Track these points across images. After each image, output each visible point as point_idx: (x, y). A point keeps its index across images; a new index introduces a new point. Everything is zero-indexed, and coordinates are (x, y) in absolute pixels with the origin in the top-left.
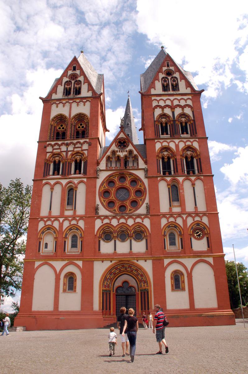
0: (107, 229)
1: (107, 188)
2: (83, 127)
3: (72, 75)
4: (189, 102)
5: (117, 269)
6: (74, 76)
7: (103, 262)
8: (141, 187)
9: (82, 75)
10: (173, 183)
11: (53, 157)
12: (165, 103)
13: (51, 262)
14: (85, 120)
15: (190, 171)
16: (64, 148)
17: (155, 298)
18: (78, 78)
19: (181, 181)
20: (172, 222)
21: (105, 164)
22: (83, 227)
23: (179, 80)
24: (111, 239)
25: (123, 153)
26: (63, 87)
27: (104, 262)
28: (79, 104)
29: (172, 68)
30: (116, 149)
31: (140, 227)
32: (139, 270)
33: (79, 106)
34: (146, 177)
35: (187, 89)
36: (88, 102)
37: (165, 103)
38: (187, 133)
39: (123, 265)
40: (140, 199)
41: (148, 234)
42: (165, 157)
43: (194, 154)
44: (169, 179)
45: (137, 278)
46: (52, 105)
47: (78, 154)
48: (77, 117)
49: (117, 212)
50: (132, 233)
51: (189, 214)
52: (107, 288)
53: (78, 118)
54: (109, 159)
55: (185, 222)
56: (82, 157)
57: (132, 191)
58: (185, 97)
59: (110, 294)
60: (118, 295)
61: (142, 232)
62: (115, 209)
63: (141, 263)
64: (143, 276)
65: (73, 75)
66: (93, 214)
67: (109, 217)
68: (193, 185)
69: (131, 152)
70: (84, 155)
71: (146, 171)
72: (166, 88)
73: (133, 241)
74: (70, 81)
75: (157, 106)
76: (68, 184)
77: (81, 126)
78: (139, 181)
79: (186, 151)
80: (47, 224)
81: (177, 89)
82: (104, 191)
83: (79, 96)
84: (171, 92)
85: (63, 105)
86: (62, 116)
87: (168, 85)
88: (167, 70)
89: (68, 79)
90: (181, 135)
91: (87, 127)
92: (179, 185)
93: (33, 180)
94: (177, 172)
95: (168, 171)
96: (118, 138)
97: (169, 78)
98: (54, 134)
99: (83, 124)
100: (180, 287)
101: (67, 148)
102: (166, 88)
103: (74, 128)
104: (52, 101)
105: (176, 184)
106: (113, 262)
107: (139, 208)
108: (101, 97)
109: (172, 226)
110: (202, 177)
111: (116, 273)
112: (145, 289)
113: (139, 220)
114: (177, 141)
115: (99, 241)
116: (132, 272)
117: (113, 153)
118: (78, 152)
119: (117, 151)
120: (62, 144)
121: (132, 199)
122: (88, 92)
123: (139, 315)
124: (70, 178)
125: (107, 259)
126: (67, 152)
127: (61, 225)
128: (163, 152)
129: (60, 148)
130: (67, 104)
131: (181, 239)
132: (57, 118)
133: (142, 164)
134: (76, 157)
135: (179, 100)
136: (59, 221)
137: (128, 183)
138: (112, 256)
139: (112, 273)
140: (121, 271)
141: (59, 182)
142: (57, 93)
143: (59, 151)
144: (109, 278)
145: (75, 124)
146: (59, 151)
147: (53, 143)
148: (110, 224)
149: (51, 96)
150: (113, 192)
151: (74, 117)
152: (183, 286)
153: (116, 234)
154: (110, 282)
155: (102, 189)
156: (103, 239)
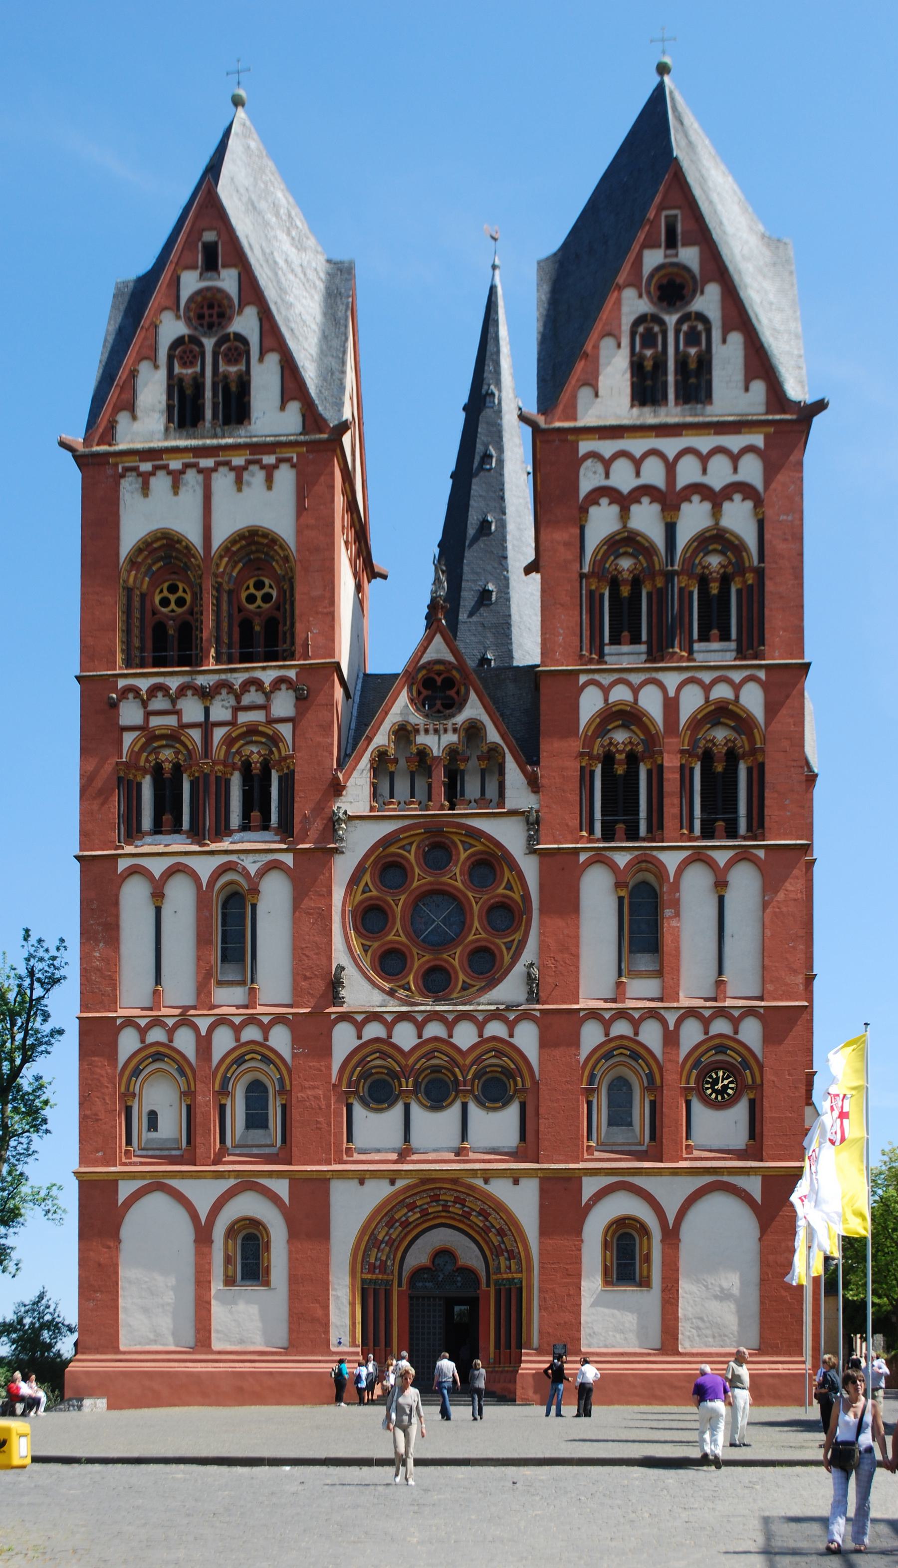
0: (379, 1062)
1: (375, 893)
2: (267, 598)
3: (199, 299)
5: (412, 1207)
6: (211, 306)
7: (362, 1182)
9: (249, 303)
10: (640, 876)
11: (149, 749)
12: (638, 474)
14: (274, 564)
15: (716, 820)
16: (192, 710)
18: (230, 319)
19: (672, 871)
20: (622, 1037)
21: (366, 791)
22: (286, 1054)
23: (716, 334)
26: (162, 374)
27: (367, 1182)
29: (689, 256)
31: (500, 1053)
32: (490, 1215)
33: (244, 488)
34: (532, 851)
35: (747, 389)
37: (638, 474)
40: (504, 943)
41: (528, 1084)
42: (618, 756)
43: (742, 743)
46: (122, 481)
47: (254, 738)
50: (469, 1077)
54: (381, 763)
56: (271, 752)
57: (476, 908)
58: (735, 442)
60: (418, 1298)
61: (509, 1074)
62: (408, 983)
63: (500, 1189)
64: (506, 1235)
65: (204, 298)
67: (385, 1016)
68: (721, 885)
70: (281, 744)
73: (474, 1110)
74: (194, 340)
75: (599, 493)
76: (220, 875)
78: (506, 869)
79: (709, 729)
82: (366, 904)
86: (172, 540)
87: (660, 364)
88: (663, 272)
92: (661, 886)
93: (76, 857)
94: (661, 827)
95: (624, 822)
96: (422, 662)
97: (671, 320)
99: (267, 581)
100: (634, 1273)
101: (207, 711)
102: (649, 383)
103: (230, 602)
104: (118, 459)
105: (651, 878)
106: (400, 1184)
107: (499, 981)
108: (346, 439)
109: (621, 1054)
111: (411, 1220)
114: (671, 681)
116: (469, 1219)
117: (401, 733)
118: (252, 730)
119: (417, 731)
122: (283, 407)
126: (207, 727)
127: (204, 1044)
128: (609, 731)
129: (178, 707)
130: (191, 476)
131: (653, 1104)
134: (247, 750)
135: (704, 460)
136: (196, 1028)
139: (397, 1221)
140: (429, 1214)
141: (187, 866)
142: (139, 413)
144: (387, 1238)
147: (144, 684)
148: (387, 1041)
150: (398, 910)
151: (226, 549)
152: (645, 1273)
154: (389, 1252)
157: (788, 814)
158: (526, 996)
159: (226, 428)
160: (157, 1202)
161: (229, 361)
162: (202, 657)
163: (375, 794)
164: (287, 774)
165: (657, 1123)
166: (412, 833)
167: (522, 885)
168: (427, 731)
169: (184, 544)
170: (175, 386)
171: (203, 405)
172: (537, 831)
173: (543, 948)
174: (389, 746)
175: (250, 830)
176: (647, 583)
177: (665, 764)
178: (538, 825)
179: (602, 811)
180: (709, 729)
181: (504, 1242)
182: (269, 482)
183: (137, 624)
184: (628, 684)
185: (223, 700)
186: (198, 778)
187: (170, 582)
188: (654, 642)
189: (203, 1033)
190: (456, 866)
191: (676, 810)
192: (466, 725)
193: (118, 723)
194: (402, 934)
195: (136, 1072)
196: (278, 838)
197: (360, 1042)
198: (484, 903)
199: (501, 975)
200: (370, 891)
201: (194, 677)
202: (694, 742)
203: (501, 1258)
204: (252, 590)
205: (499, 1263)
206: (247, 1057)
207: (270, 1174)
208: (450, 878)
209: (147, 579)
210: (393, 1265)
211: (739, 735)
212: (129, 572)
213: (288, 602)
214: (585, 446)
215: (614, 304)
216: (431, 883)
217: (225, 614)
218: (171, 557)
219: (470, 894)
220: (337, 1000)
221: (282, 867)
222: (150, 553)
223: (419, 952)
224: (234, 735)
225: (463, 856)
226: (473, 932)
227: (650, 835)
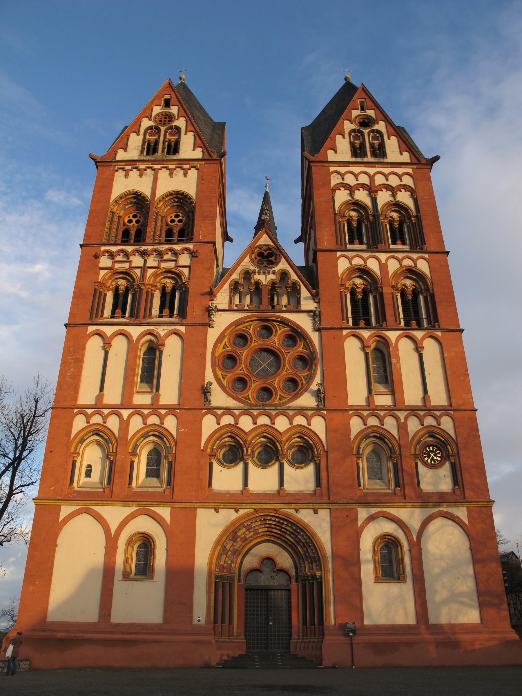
4: (408, 181)
11: (113, 279)
13: (97, 508)
14: (185, 207)
15: (411, 320)
16: (137, 261)
22: (173, 431)
23: (385, 137)
26: (141, 137)
28: (175, 172)
29: (371, 113)
30: (252, 268)
33: (174, 176)
34: (317, 329)
44: (366, 334)
46: (116, 173)
48: (168, 200)
50: (285, 448)
51: (413, 411)
54: (235, 287)
55: (402, 427)
56: (177, 282)
58: (400, 171)
59: (231, 586)
64: (310, 547)
66: (198, 404)
68: (419, 349)
69: (284, 275)
70: (183, 277)
75: (338, 186)
76: (144, 336)
77: (177, 220)
83: (175, 157)
84: (369, 159)
87: (363, 145)
89: (151, 123)
90: (391, 247)
91: (189, 220)
94: (384, 319)
97: (366, 131)
103: (162, 221)
104: (116, 164)
106: (242, 512)
113: (300, 420)
115: (211, 464)
118: (168, 271)
119: (254, 272)
120: (134, 253)
122: (194, 150)
126: (144, 269)
129: (130, 260)
132: (126, 200)
133: (308, 304)
135: (386, 176)
136: (120, 416)
137: (277, 342)
142: (128, 150)
143: (127, 266)
146: (127, 266)
147: (114, 249)
148: (235, 426)
149: (116, 154)
150: (243, 357)
155: (220, 350)
160: (85, 519)
161: (171, 134)
171: (158, 148)
177: (384, 292)
178: (320, 317)
179: (352, 313)
181: (308, 552)
182: (185, 175)
183: (115, 227)
187: (134, 214)
191: (393, 312)
192: (280, 272)
193: (98, 265)
195: (82, 441)
197: (219, 426)
201: (140, 246)
206: (150, 434)
210: (235, 567)
212: (114, 206)
214: (332, 169)
220: (207, 400)
222: (126, 200)
224: (158, 273)
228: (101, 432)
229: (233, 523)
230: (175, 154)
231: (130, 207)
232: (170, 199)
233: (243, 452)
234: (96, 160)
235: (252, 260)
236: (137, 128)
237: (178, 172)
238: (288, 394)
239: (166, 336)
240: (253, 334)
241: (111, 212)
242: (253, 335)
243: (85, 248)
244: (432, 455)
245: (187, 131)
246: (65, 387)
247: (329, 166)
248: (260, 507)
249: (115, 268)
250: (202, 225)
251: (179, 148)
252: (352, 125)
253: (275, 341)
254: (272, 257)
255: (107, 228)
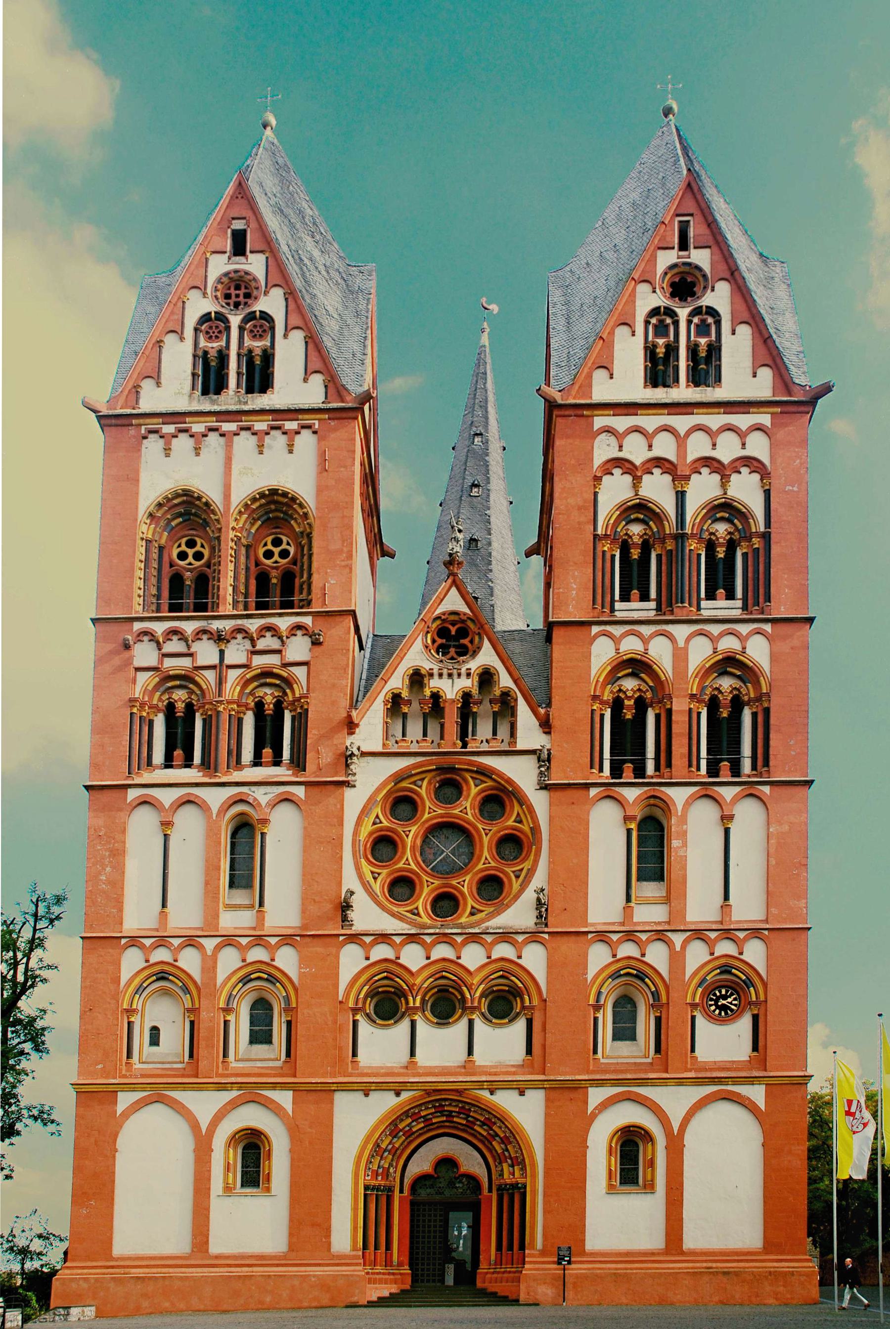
1: (386, 823)
3: (225, 280)
5: (416, 1117)
6: (238, 288)
7: (367, 1095)
8: (521, 822)
11: (162, 689)
14: (292, 522)
15: (722, 760)
16: (207, 653)
17: (545, 1212)
20: (629, 958)
22: (293, 973)
24: (399, 1015)
25: (456, 680)
30: (427, 664)
33: (265, 450)
34: (544, 787)
36: (305, 433)
38: (730, 595)
39: (441, 1105)
41: (536, 1002)
42: (626, 702)
44: (631, 794)
45: (487, 1147)
46: (145, 441)
47: (268, 680)
48: (257, 508)
49: (425, 920)
50: (478, 994)
52: (380, 1181)
53: (261, 511)
54: (396, 703)
56: (285, 694)
57: (486, 840)
58: (743, 421)
61: (515, 992)
62: (417, 908)
68: (726, 819)
70: (295, 686)
71: (544, 759)
72: (661, 367)
80: (153, 960)
81: (712, 371)
82: (375, 836)
85: (191, 442)
86: (192, 496)
87: (672, 350)
88: (676, 271)
91: (303, 555)
92: (669, 819)
94: (669, 765)
95: (631, 761)
98: (159, 580)
99: (285, 539)
100: (637, 1178)
101: (222, 652)
103: (247, 557)
104: (141, 421)
105: (658, 813)
106: (405, 1095)
110: (766, 789)
111: (414, 1129)
112: (515, 1186)
113: (503, 950)
114: (681, 632)
115: (355, 1023)
119: (431, 675)
121: (482, 870)
122: (305, 380)
123: (490, 1264)
124: (238, 784)
125: (381, 1087)
126: (221, 667)
128: (620, 678)
129: (192, 650)
131: (658, 1020)
134: (260, 692)
138: (399, 1074)
139: (401, 1130)
141: (197, 796)
143: (186, 662)
144: (390, 1146)
145: (250, 539)
146: (186, 662)
147: (159, 628)
148: (395, 962)
150: (409, 841)
152: (649, 1177)
153: (418, 999)
154: (392, 1160)
155: (367, 828)
156: (368, 1016)
157: (793, 753)
158: (535, 920)
159: (250, 395)
162: (218, 604)
163: (387, 735)
164: (300, 713)
165: (663, 1037)
166: (424, 769)
167: (532, 818)
168: (441, 675)
169: (204, 500)
170: (202, 358)
171: (227, 374)
172: (548, 768)
173: (552, 876)
174: (402, 689)
175: (261, 765)
176: (656, 546)
177: (674, 708)
178: (549, 763)
180: (717, 677)
181: (507, 1150)
184: (639, 635)
185: (239, 644)
186: (211, 716)
188: (664, 599)
189: (209, 953)
190: (467, 800)
191: (685, 750)
192: (480, 670)
194: (412, 863)
196: (290, 772)
197: (368, 963)
198: (495, 834)
199: (510, 901)
200: (381, 822)
201: (210, 622)
202: (702, 689)
203: (505, 1166)
204: (270, 547)
205: (502, 1170)
206: (253, 976)
207: (274, 1086)
208: (461, 811)
209: (166, 534)
211: (744, 683)
213: (306, 558)
214: (599, 422)
215: (630, 295)
216: (441, 816)
217: (243, 566)
218: (190, 514)
219: (480, 826)
221: (293, 799)
222: (170, 509)
223: (429, 879)
224: (248, 676)
225: (474, 790)
226: (482, 861)
227: (657, 773)
228: (170, 975)
229: (392, 1111)
230: (265, 393)
231: (180, 523)
232: (261, 506)
233: (407, 1003)
234: (100, 412)
235: (427, 647)
236: (178, 320)
237: (275, 439)
238: (486, 904)
239: (270, 805)
240: (427, 795)
241: (142, 539)
242: (428, 798)
243: (103, 627)
244: (724, 1002)
245: (289, 329)
246: (99, 900)
247: (593, 416)
248: (433, 1088)
249: (164, 667)
250: (329, 571)
251: (273, 373)
252: (654, 294)
253: (466, 808)
254: (465, 637)
255: (140, 578)
